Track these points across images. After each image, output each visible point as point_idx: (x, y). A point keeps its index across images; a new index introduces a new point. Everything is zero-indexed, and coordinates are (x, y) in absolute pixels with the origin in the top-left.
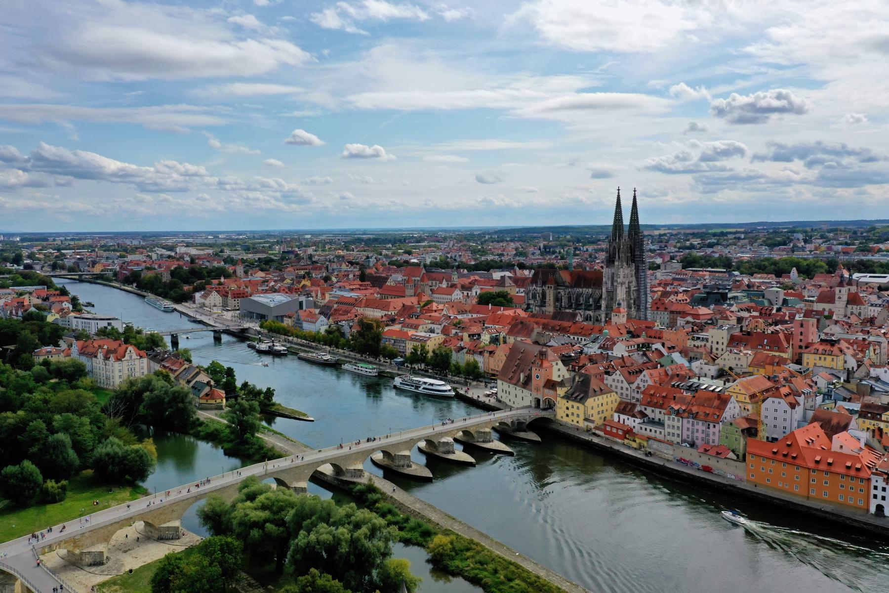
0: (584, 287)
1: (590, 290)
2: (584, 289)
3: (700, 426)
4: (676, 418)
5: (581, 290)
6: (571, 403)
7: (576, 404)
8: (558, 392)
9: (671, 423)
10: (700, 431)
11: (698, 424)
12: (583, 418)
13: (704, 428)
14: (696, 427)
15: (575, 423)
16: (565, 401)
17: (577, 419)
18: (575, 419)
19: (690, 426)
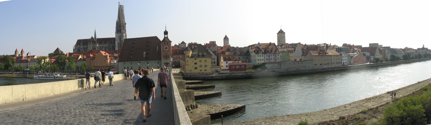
0: (104, 43)
1: (107, 45)
2: (104, 45)
3: (272, 57)
5: (102, 45)
6: (198, 60)
7: (203, 59)
8: (187, 55)
10: (272, 59)
11: (271, 55)
14: (271, 57)
15: (203, 71)
17: (206, 68)
19: (268, 57)
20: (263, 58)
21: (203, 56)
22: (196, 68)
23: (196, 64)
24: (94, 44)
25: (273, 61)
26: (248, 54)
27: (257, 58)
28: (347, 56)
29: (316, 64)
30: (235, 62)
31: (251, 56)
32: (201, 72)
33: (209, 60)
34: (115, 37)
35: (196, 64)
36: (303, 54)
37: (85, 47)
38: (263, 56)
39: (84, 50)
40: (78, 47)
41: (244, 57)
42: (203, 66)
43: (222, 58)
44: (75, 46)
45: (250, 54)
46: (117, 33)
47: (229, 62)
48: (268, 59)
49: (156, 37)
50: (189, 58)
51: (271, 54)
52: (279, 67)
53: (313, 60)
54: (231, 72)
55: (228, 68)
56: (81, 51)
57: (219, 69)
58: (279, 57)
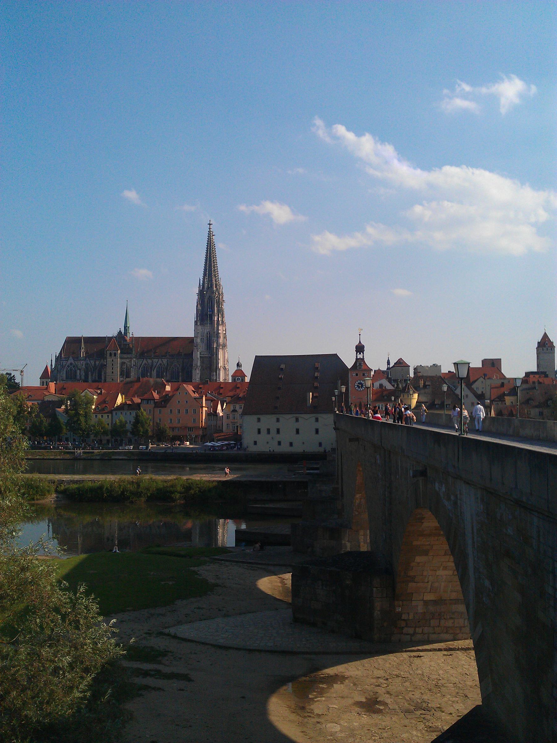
2: (155, 360)
5: (150, 361)
24: (125, 356)
34: (192, 335)
37: (93, 364)
39: (92, 375)
40: (69, 362)
44: (57, 359)
46: (200, 325)
49: (335, 357)
56: (78, 377)
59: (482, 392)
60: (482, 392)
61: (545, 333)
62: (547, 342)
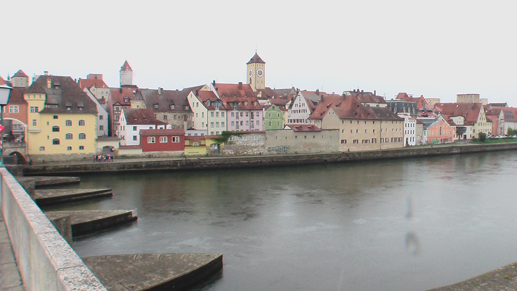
3: (245, 118)
4: (220, 112)
6: (62, 119)
7: (75, 118)
9: (214, 119)
10: (244, 123)
12: (96, 137)
13: (248, 118)
15: (76, 150)
16: (49, 118)
17: (82, 142)
18: (76, 143)
19: (234, 119)
20: (224, 119)
21: (75, 109)
22: (56, 142)
23: (56, 129)
25: (244, 128)
26: (187, 108)
27: (212, 119)
28: (415, 123)
29: (344, 140)
30: (156, 127)
31: (195, 114)
32: (70, 152)
33: (90, 120)
35: (56, 129)
36: (311, 114)
38: (223, 115)
41: (178, 114)
42: (76, 136)
43: (122, 116)
45: (190, 108)
47: (140, 127)
48: (235, 123)
50: (38, 113)
51: (241, 112)
52: (262, 143)
53: (339, 130)
54: (147, 153)
55: (137, 143)
57: (115, 145)
58: (260, 118)
59: (103, 97)
60: (103, 97)
61: (126, 61)
62: (127, 67)
